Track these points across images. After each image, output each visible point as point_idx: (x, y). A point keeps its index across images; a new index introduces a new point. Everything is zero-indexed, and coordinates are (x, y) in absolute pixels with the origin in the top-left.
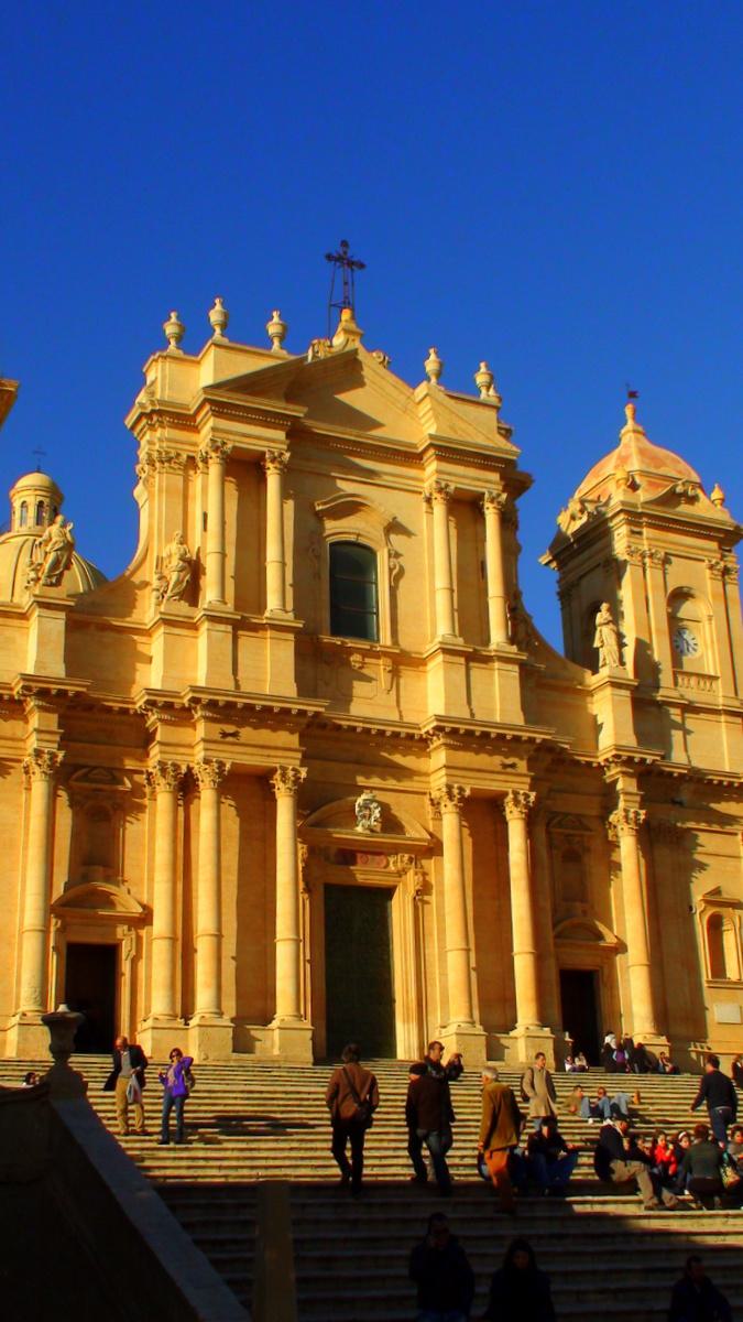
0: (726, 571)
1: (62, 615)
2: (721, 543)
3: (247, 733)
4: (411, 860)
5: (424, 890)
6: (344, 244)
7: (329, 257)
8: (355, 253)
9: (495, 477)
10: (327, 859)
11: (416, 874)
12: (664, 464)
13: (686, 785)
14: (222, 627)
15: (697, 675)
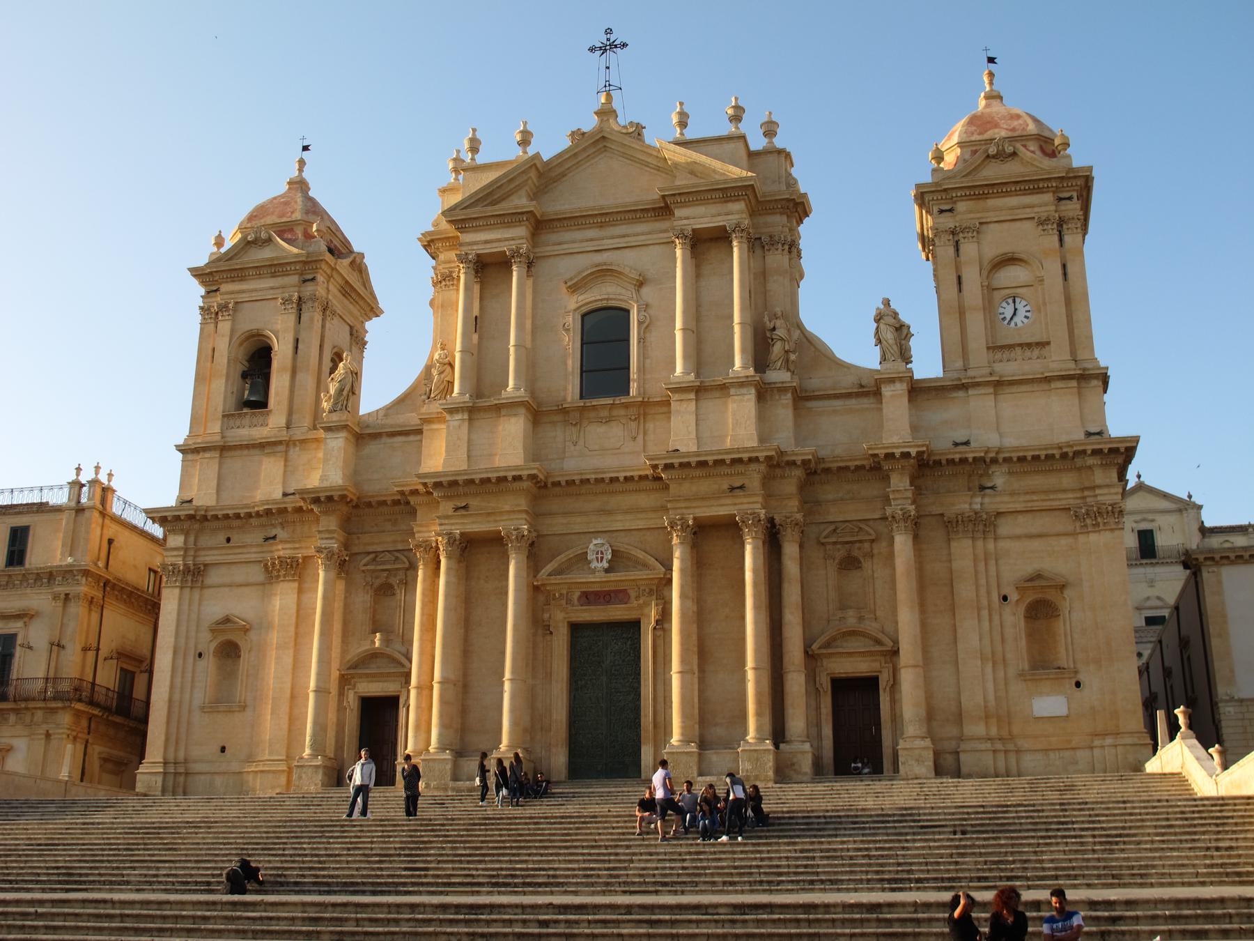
0: (1061, 223)
1: (343, 434)
2: (1056, 190)
3: (474, 503)
4: (651, 590)
5: (665, 616)
6: (609, 31)
7: (592, 49)
8: (617, 37)
9: (740, 206)
10: (569, 601)
11: (657, 605)
12: (996, 126)
13: (994, 468)
14: (459, 416)
15: (1021, 345)
